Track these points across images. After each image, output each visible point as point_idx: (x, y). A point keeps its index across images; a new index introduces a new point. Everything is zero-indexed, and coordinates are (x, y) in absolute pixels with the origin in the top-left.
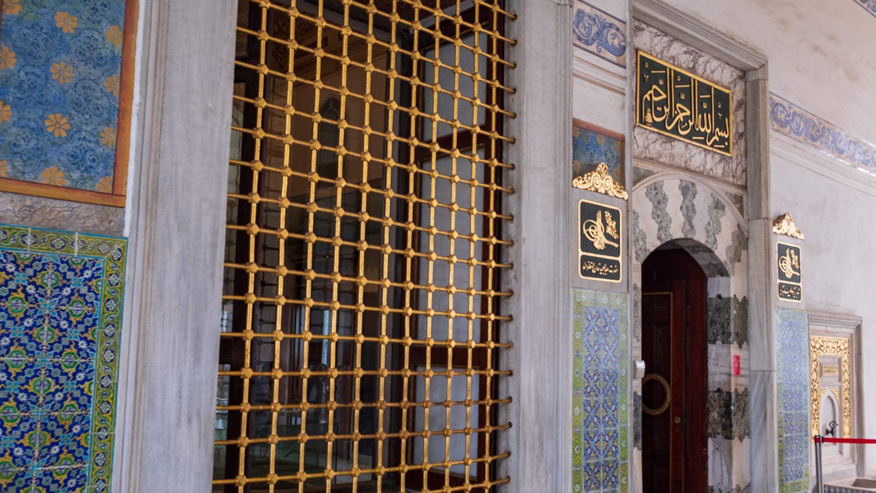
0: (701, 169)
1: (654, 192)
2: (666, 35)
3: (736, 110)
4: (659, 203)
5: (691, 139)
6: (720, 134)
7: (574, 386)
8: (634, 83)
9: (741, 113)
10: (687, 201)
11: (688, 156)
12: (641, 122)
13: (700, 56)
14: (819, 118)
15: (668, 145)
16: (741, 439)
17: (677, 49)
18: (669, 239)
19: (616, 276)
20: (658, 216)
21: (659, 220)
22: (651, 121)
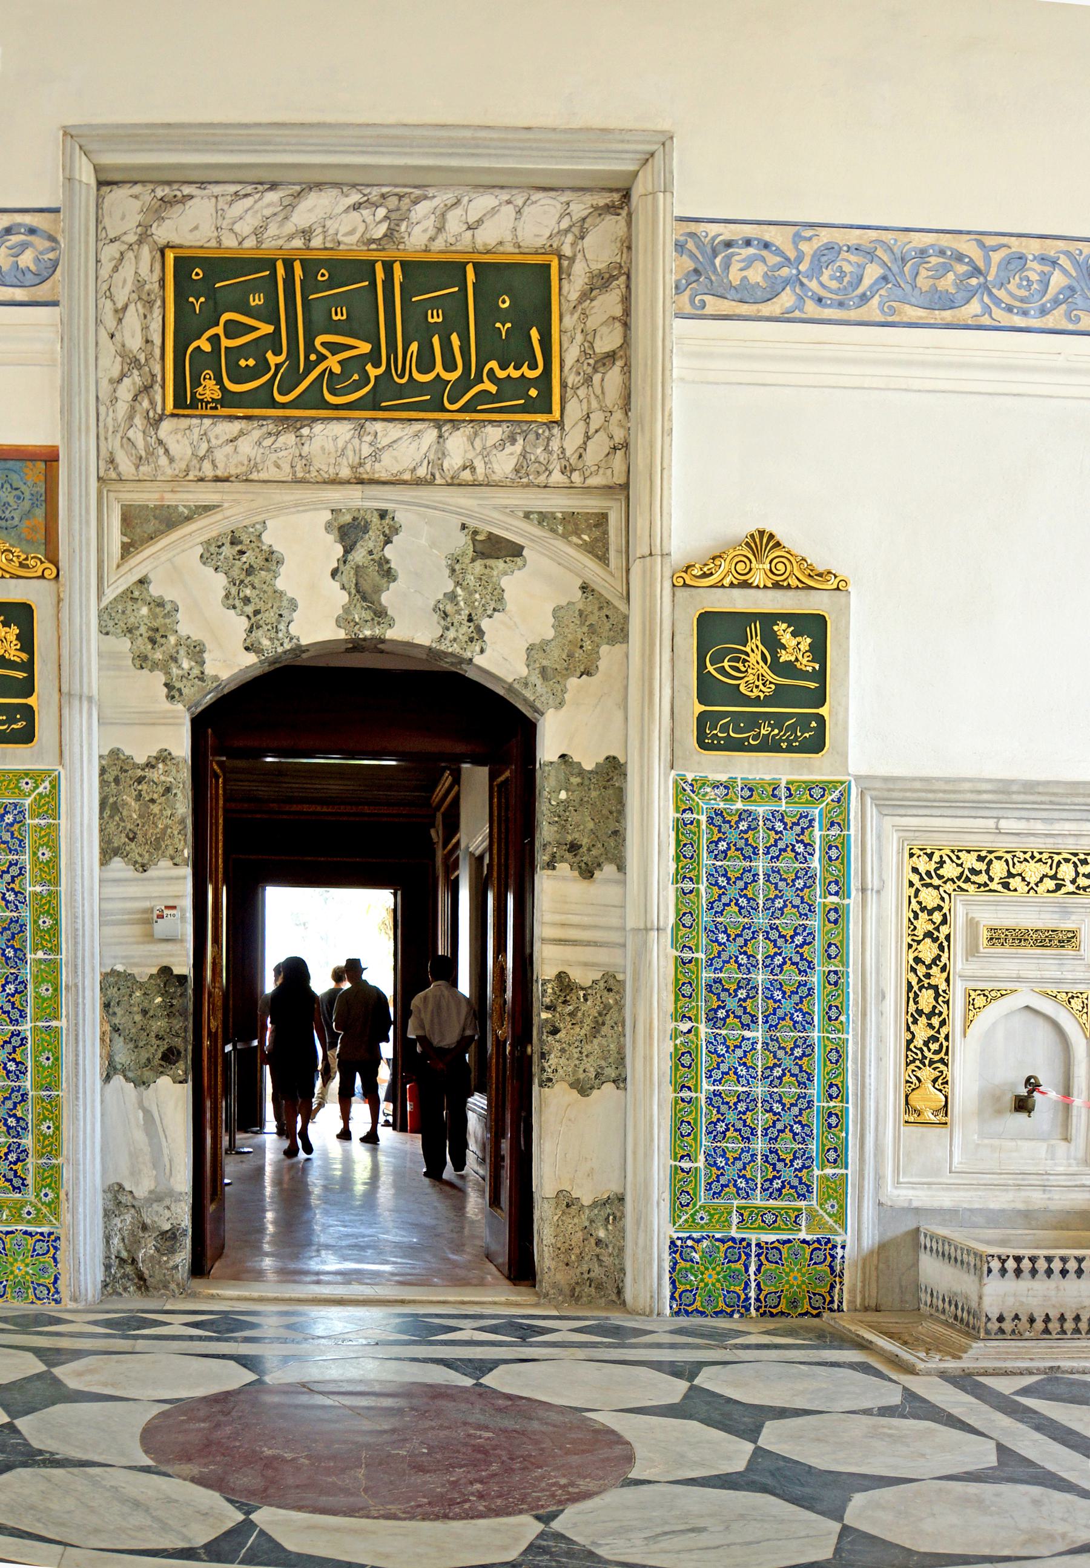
0: (422, 472)
1: (228, 551)
2: (274, 186)
3: (587, 295)
4: (250, 571)
5: (376, 407)
6: (501, 374)
7: (101, 989)
8: (155, 326)
9: (609, 303)
10: (359, 556)
11: (366, 450)
12: (180, 401)
13: (415, 202)
14: (979, 236)
15: (288, 439)
16: (583, 1089)
17: (312, 209)
18: (287, 646)
19: (27, 736)
20: (247, 601)
21: (249, 610)
22: (217, 395)
